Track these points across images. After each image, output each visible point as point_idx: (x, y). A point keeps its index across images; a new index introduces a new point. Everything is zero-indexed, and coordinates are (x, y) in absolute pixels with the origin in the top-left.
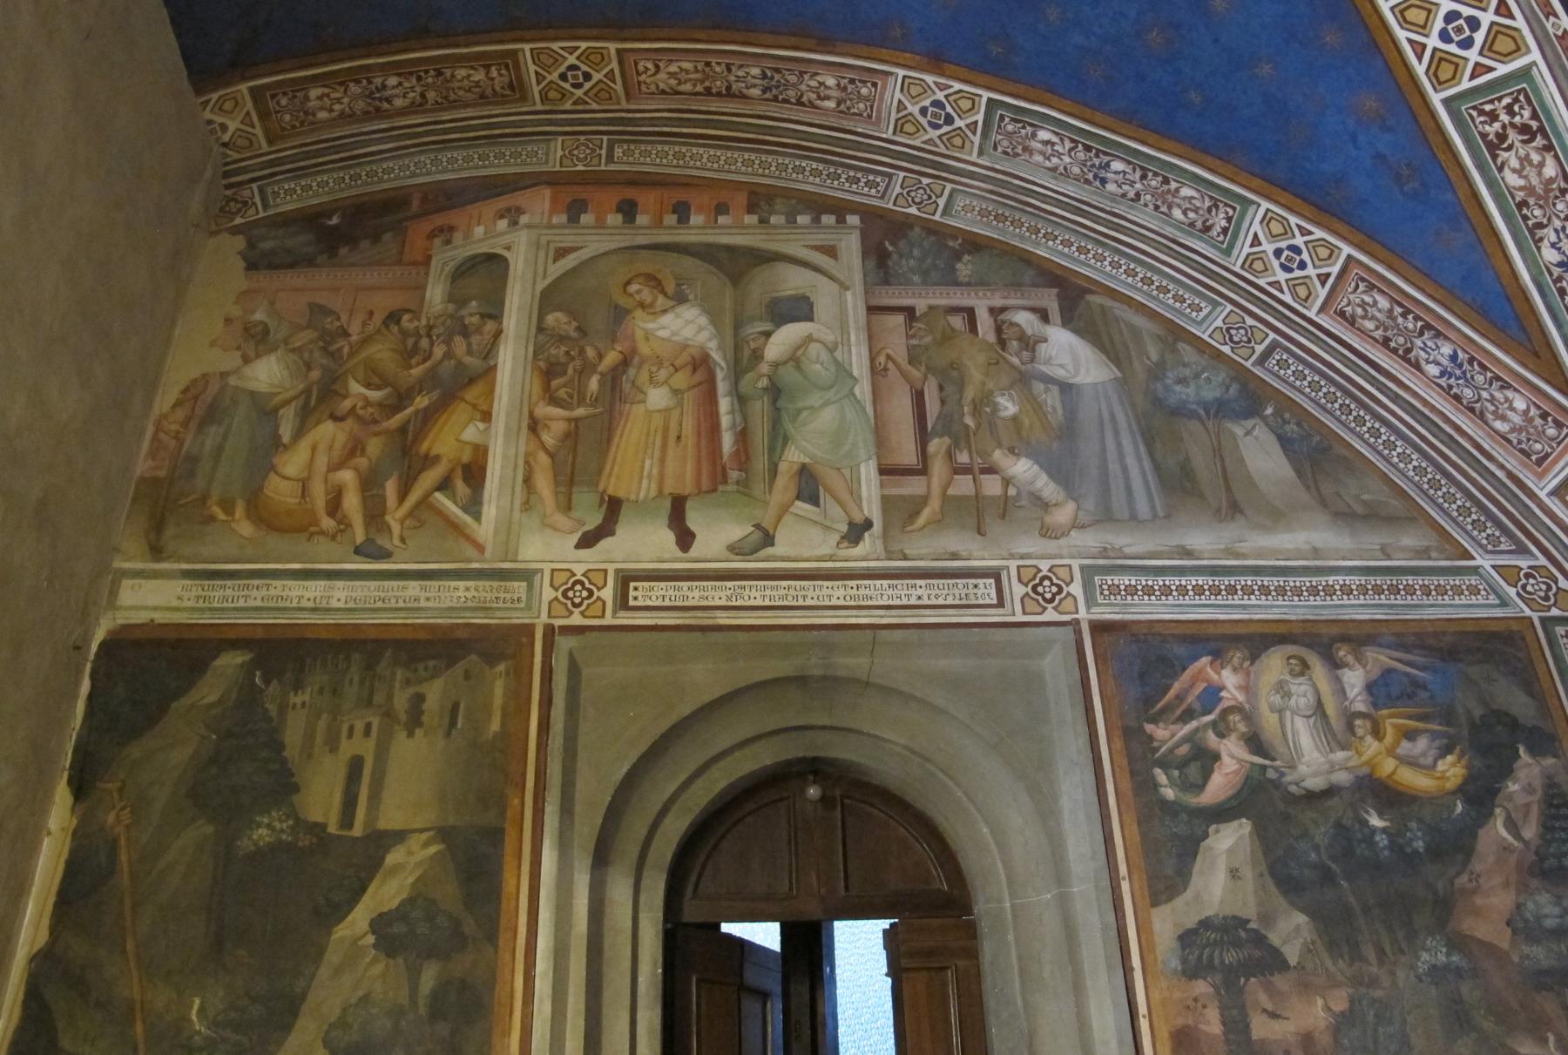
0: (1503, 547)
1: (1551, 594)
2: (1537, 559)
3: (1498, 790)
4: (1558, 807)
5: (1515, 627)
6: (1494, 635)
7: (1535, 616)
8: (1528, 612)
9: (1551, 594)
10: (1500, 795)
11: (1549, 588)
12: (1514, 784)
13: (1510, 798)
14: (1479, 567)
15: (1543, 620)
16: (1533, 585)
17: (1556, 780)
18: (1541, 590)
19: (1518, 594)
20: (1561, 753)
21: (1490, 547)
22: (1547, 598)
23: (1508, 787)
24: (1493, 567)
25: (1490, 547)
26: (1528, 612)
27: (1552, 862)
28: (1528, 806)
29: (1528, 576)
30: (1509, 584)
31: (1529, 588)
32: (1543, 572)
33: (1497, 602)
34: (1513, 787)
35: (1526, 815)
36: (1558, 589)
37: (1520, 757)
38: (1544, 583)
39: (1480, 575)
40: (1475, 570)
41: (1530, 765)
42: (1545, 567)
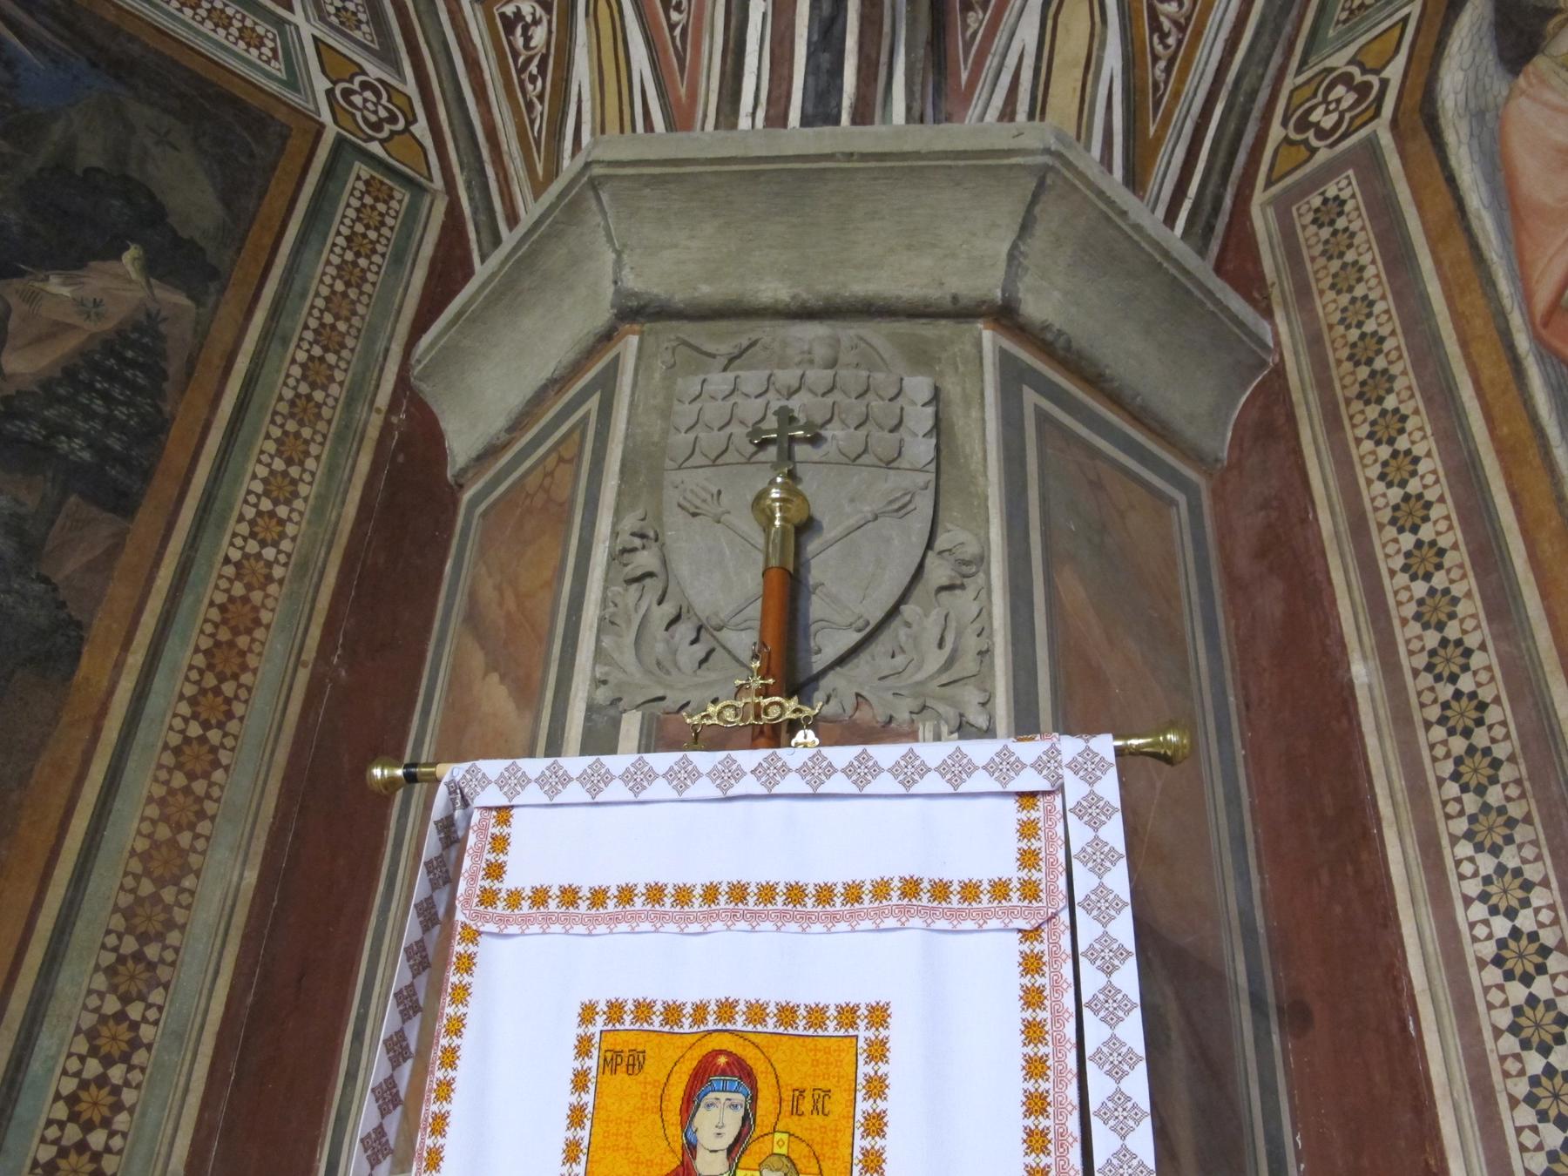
0: (358, 35)
1: (387, 128)
2: (404, 80)
3: (20, 274)
4: (132, 364)
5: (281, 115)
6: (234, 101)
7: (331, 132)
8: (326, 116)
9: (387, 128)
10: (17, 283)
11: (393, 119)
12: (64, 284)
13: (32, 297)
14: (290, 23)
15: (340, 142)
16: (365, 100)
17: (163, 328)
18: (375, 112)
19: (330, 93)
20: (211, 301)
21: (334, 20)
22: (377, 127)
23: (46, 279)
24: (315, 39)
25: (334, 20)
26: (326, 116)
27: (34, 431)
28: (59, 329)
29: (365, 86)
30: (324, 72)
31: (357, 100)
32: (398, 100)
33: (284, 77)
34: (56, 286)
35: (39, 340)
36: (406, 130)
37: (118, 257)
38: (385, 108)
39: (282, 33)
40: (280, 23)
41: (130, 281)
42: (409, 99)
